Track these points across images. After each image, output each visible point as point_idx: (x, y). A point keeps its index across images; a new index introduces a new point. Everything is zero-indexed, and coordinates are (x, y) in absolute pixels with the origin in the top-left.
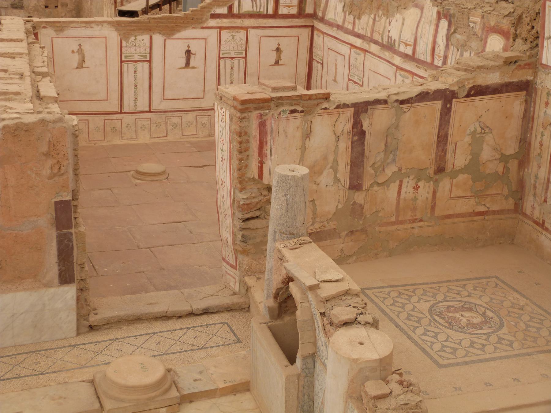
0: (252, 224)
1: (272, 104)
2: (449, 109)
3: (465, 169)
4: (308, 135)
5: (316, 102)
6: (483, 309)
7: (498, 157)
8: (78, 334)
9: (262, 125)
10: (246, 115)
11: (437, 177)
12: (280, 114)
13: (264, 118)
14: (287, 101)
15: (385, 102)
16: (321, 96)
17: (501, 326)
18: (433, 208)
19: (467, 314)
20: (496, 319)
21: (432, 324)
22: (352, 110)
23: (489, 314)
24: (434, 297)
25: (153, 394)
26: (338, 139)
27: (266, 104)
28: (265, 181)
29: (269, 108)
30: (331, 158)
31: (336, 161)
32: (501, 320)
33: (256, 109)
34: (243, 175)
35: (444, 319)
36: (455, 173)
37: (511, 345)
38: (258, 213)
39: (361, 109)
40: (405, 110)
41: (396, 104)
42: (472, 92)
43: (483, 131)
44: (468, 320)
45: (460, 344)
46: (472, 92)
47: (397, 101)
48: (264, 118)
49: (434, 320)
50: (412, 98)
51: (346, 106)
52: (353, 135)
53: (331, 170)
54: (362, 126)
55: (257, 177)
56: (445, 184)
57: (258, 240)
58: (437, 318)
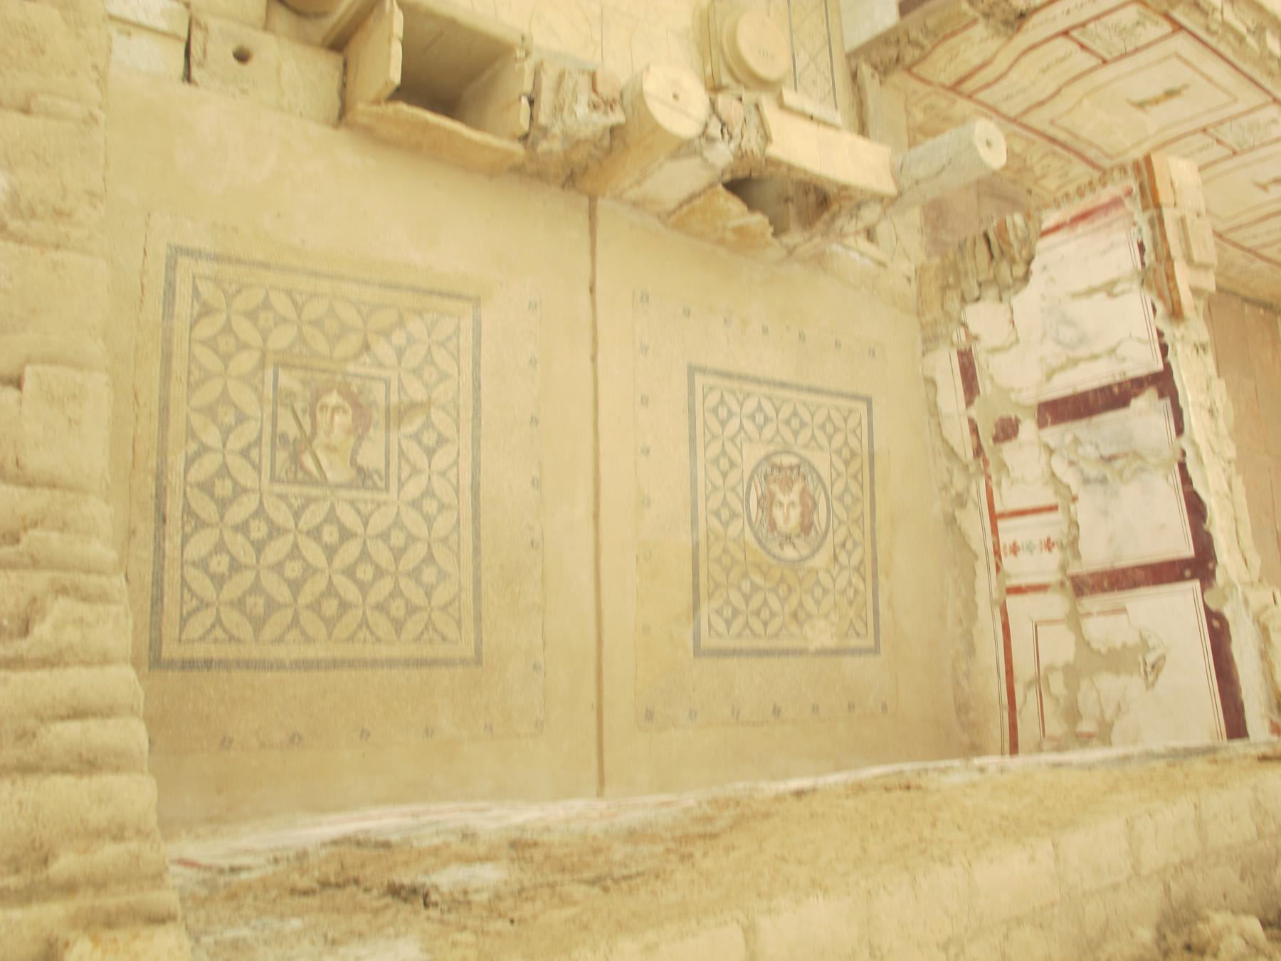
0: (982, 246)
1: (1152, 212)
2: (1180, 578)
3: (1083, 643)
4: (1109, 289)
5: (1166, 293)
6: (805, 552)
7: (1109, 714)
8: (852, 56)
9: (1116, 203)
10: (1130, 172)
11: (1068, 584)
12: (1135, 224)
13: (1127, 201)
14: (1159, 238)
15: (1180, 430)
16: (1175, 298)
17: (760, 542)
18: (1017, 590)
19: (795, 514)
20: (777, 551)
21: (778, 439)
22: (1159, 366)
23: (789, 553)
24: (840, 499)
25: (726, 48)
26: (1112, 351)
27: (1151, 201)
28: (1041, 245)
29: (1145, 208)
30: (1082, 352)
31: (1074, 362)
32: (774, 556)
33: (1141, 187)
34: (1046, 206)
35: (791, 468)
36: (1075, 621)
37: (717, 514)
38: (996, 252)
39: (1163, 382)
40: (1170, 479)
41: (1178, 456)
42: (1216, 624)
43: (1149, 669)
44: (781, 504)
45: (732, 440)
46: (1216, 624)
47: (1184, 454)
48: (1127, 201)
49: (789, 452)
50: (1191, 483)
51: (1164, 349)
52: (1120, 385)
53: (1064, 359)
54: (1136, 395)
55: (1045, 226)
56: (1056, 604)
57: (961, 266)
58: (793, 460)
